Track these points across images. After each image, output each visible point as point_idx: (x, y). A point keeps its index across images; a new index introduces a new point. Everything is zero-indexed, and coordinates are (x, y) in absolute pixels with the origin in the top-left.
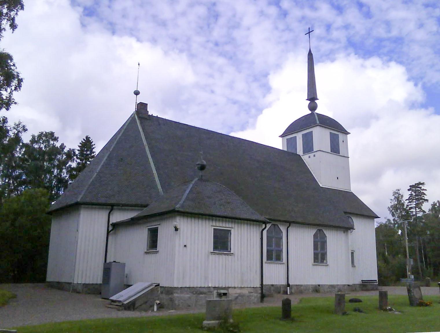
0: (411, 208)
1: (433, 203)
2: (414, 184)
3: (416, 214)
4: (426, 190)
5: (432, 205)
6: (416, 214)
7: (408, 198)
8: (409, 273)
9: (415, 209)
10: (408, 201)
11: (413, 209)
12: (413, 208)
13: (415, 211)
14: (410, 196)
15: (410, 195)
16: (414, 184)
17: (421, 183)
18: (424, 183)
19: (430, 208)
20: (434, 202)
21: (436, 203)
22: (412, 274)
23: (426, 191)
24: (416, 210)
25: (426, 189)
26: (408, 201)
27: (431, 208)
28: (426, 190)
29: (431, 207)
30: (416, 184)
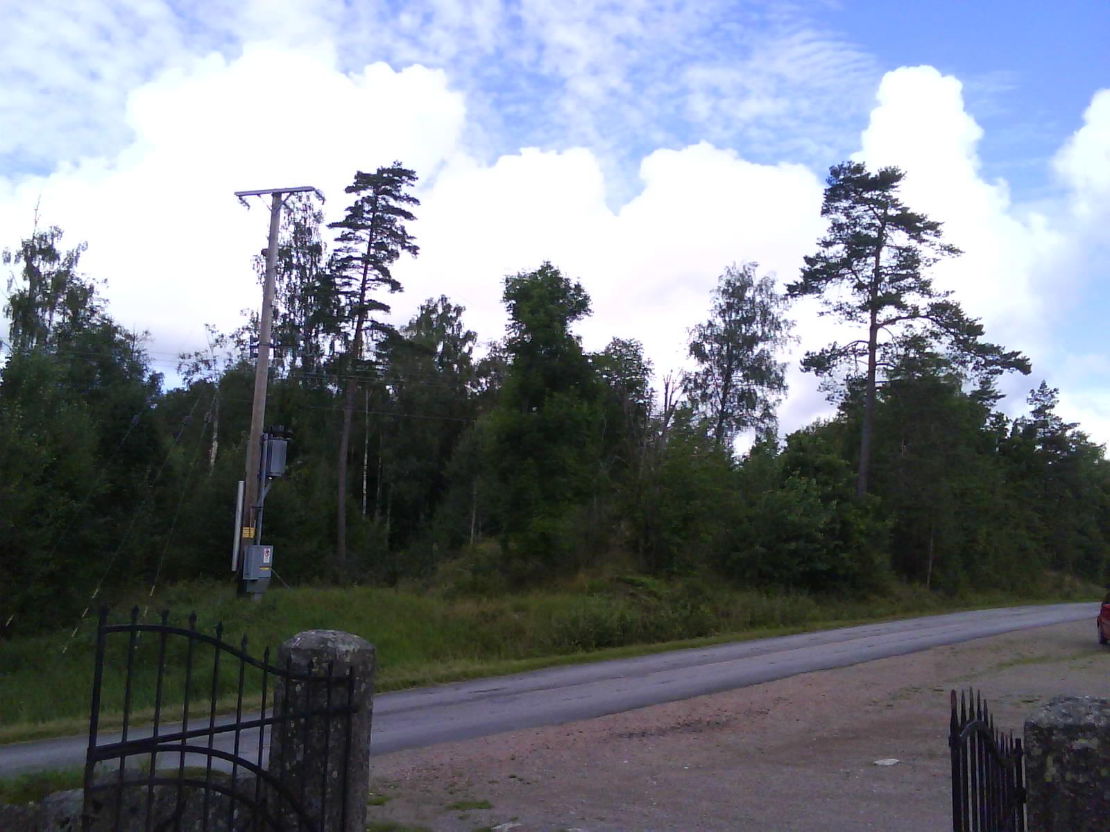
0: (346, 263)
1: (425, 304)
2: (375, 172)
3: (363, 289)
4: (416, 201)
5: (422, 308)
6: (363, 289)
7: (341, 219)
8: (249, 533)
9: (362, 270)
10: (338, 232)
11: (354, 271)
12: (355, 262)
13: (361, 277)
14: (349, 213)
15: (350, 208)
16: (375, 172)
17: (404, 167)
18: (413, 172)
19: (416, 319)
20: (430, 301)
21: (436, 305)
22: (267, 537)
23: (415, 206)
24: (365, 275)
25: (417, 198)
26: (338, 232)
27: (417, 321)
28: (416, 201)
29: (419, 316)
30: (381, 171)
